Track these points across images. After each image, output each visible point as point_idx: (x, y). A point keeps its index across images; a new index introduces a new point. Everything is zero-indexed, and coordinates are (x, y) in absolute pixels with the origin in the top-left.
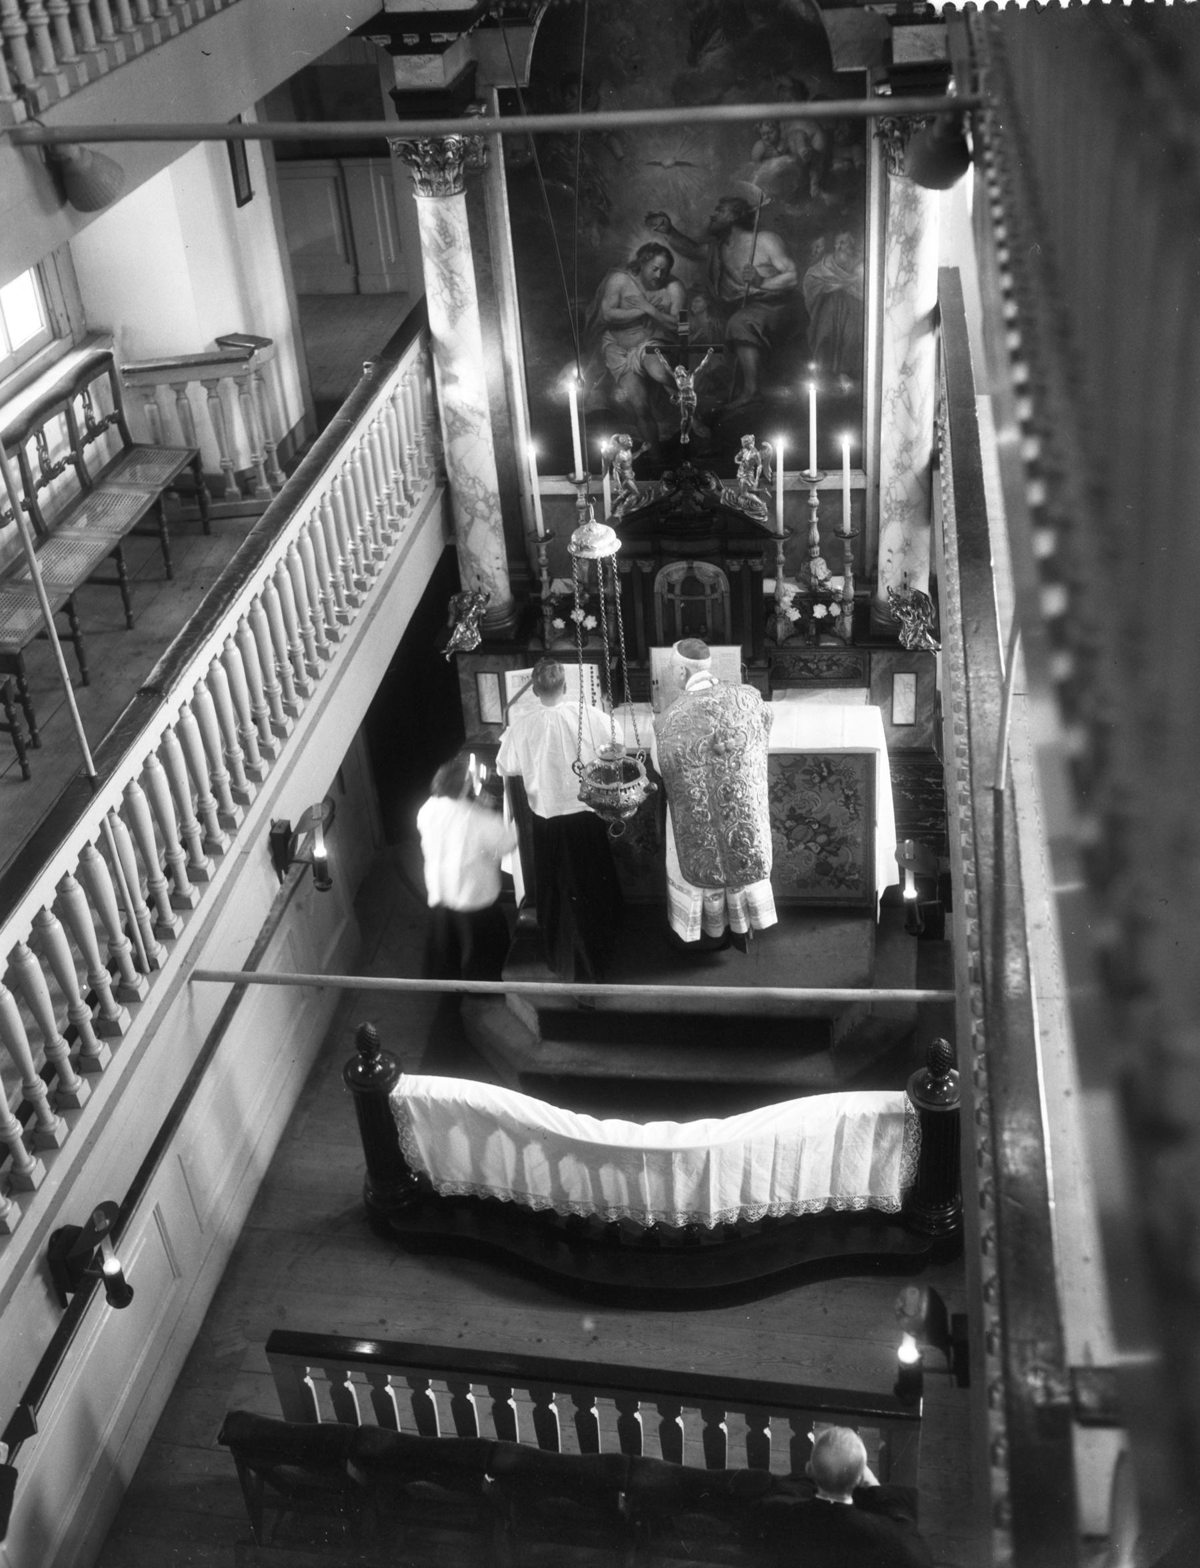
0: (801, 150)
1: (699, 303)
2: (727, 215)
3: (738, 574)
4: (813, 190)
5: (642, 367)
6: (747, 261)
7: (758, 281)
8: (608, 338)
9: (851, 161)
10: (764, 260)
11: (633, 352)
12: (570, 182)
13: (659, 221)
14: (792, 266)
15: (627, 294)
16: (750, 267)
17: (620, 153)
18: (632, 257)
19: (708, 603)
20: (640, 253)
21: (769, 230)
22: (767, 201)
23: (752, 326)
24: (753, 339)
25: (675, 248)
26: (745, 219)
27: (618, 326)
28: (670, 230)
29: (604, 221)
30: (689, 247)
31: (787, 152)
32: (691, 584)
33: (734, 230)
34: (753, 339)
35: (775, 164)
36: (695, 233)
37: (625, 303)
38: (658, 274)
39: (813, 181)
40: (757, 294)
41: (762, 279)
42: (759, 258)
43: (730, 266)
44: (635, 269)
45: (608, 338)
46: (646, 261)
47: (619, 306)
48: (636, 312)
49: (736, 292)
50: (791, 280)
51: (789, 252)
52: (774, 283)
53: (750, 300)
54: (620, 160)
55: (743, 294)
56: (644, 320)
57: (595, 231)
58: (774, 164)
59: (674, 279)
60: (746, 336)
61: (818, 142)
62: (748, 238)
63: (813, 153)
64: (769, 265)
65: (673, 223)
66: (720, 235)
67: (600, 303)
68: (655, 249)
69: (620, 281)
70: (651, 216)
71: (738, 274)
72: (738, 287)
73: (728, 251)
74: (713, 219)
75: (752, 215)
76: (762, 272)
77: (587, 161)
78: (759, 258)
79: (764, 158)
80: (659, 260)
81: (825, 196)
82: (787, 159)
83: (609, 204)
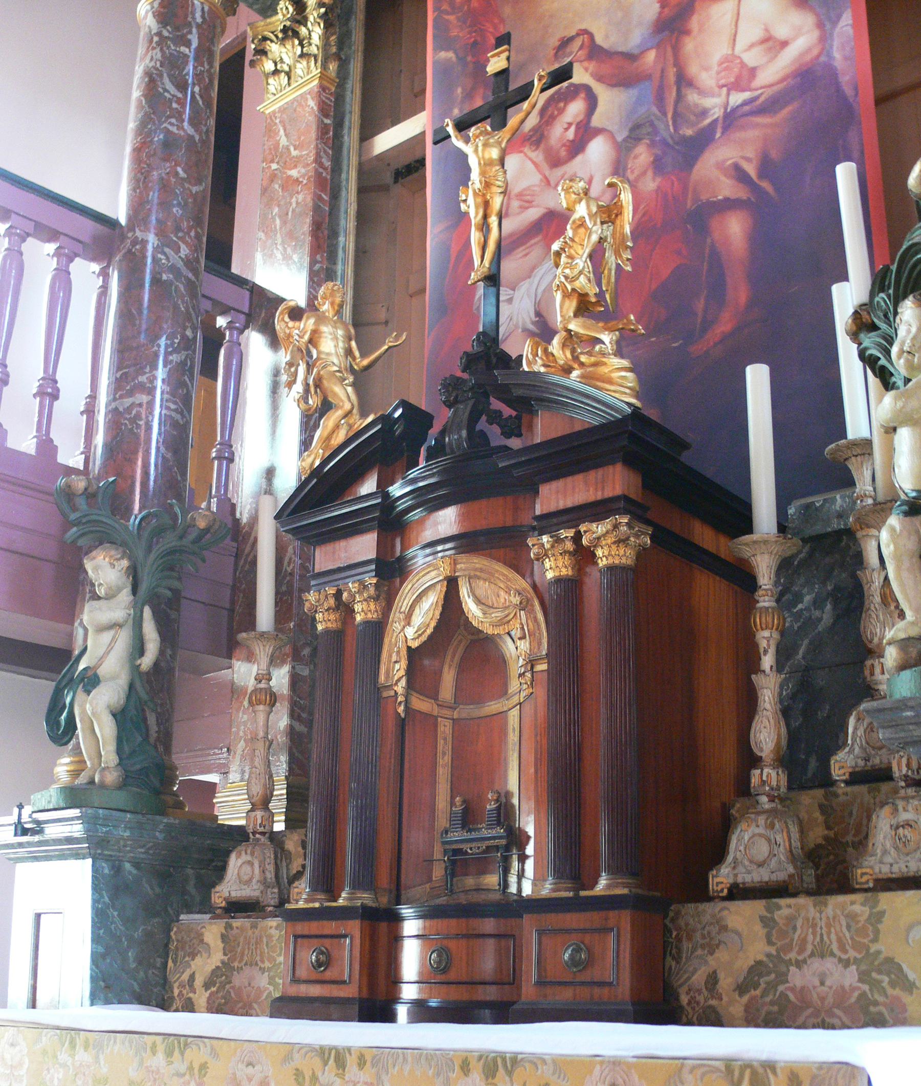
1: (642, 156)
5: (538, 314)
7: (743, 77)
10: (757, 33)
13: (578, 43)
23: (737, 167)
25: (600, 79)
30: (620, 68)
38: (571, 134)
40: (745, 103)
41: (753, 72)
43: (693, 69)
49: (704, 113)
50: (809, 50)
55: (717, 113)
59: (598, 131)
60: (727, 189)
65: (599, 40)
71: (707, 79)
72: (708, 102)
76: (751, 58)
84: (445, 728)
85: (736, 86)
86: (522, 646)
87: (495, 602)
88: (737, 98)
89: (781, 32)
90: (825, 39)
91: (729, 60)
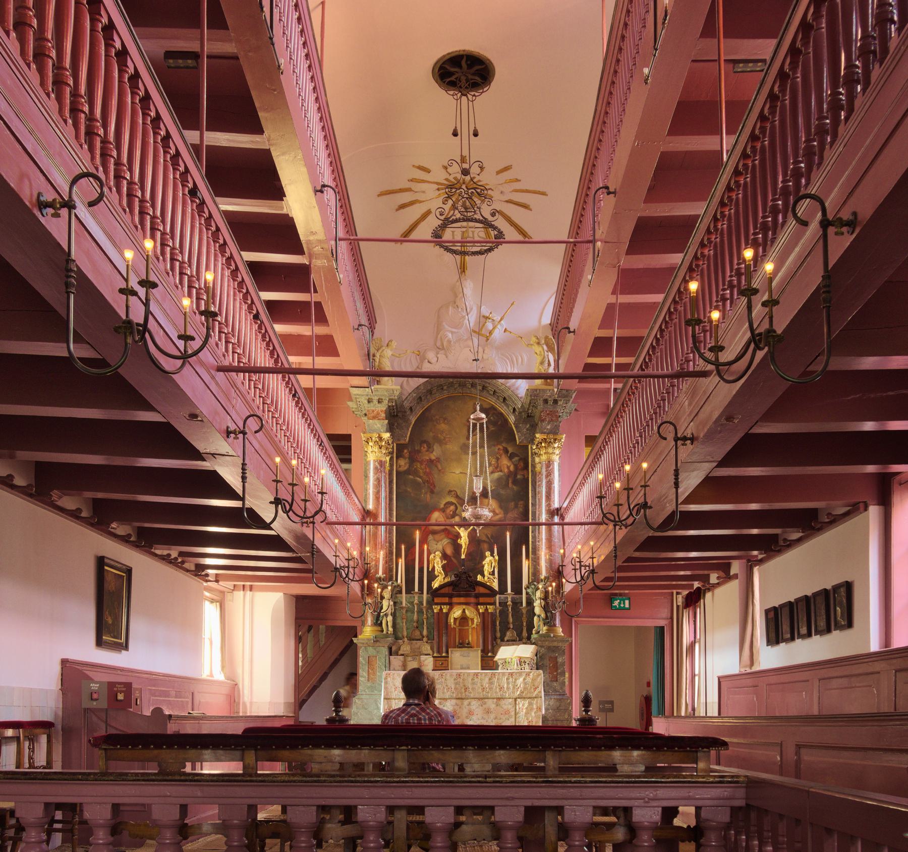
0: (506, 470)
4: (510, 485)
8: (430, 537)
12: (420, 477)
18: (442, 506)
28: (457, 497)
29: (432, 492)
32: (464, 619)
35: (496, 475)
44: (443, 510)
45: (430, 537)
51: (501, 507)
60: (484, 538)
61: (512, 468)
63: (510, 472)
68: (452, 503)
70: (450, 491)
80: (452, 508)
89: (497, 511)
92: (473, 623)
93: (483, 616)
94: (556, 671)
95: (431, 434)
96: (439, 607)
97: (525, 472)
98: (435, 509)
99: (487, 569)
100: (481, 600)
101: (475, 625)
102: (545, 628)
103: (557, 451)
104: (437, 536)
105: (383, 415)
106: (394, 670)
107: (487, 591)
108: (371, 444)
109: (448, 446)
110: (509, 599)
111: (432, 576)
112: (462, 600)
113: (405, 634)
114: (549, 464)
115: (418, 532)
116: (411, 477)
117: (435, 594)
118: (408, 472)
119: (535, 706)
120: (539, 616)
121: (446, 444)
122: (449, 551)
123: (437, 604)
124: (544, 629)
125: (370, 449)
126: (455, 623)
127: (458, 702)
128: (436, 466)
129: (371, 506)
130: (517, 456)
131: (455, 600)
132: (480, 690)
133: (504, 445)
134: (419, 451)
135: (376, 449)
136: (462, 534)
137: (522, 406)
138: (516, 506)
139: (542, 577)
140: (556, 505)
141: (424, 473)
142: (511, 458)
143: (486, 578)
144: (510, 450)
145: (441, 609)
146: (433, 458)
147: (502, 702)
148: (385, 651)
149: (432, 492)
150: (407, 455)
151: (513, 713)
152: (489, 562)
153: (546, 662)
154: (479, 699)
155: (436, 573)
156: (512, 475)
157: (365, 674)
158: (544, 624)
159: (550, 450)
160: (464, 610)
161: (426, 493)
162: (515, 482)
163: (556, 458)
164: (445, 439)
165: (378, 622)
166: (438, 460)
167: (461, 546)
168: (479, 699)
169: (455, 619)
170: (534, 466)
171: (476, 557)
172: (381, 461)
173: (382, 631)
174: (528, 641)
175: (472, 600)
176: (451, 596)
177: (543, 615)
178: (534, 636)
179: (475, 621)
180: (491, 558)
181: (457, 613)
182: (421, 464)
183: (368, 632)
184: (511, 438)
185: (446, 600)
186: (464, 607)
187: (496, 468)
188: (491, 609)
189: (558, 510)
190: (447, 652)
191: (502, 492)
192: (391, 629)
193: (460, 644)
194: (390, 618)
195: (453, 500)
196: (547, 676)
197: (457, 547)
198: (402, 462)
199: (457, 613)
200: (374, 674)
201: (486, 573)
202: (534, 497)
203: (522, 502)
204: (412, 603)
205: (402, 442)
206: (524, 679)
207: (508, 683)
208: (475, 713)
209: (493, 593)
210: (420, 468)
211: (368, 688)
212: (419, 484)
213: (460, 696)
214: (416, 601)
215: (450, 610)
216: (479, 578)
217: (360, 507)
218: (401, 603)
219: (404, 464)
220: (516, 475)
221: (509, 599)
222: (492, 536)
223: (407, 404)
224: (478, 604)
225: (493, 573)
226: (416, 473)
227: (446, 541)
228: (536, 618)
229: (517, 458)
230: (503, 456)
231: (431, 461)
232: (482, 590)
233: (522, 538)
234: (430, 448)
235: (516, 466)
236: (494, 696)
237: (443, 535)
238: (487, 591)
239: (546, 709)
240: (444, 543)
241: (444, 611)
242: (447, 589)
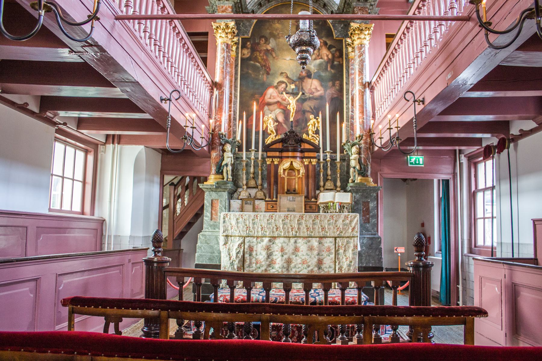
0: (326, 58)
2: (304, 73)
3: (308, 165)
4: (329, 69)
6: (309, 87)
8: (266, 108)
9: (339, 62)
10: (315, 87)
11: (273, 112)
12: (259, 62)
14: (323, 89)
15: (273, 95)
16: (310, 89)
17: (274, 55)
18: (275, 84)
19: (297, 179)
20: (278, 83)
21: (316, 79)
22: (316, 71)
24: (311, 110)
26: (309, 76)
27: (269, 104)
28: (287, 77)
29: (268, 74)
31: (322, 58)
33: (306, 78)
34: (311, 110)
35: (318, 61)
36: (295, 79)
37: (272, 97)
38: (283, 89)
39: (329, 67)
41: (314, 93)
42: (313, 87)
44: (276, 87)
45: (266, 108)
46: (279, 85)
47: (270, 98)
48: (275, 100)
51: (322, 85)
52: (317, 94)
53: (310, 98)
54: (274, 58)
56: (278, 102)
57: (265, 76)
58: (318, 61)
60: (308, 109)
61: (330, 56)
62: (309, 81)
63: (329, 59)
64: (316, 89)
66: (301, 79)
67: (264, 97)
68: (283, 82)
69: (271, 91)
70: (282, 73)
73: (304, 84)
74: (300, 75)
75: (311, 75)
76: (314, 90)
77: (265, 57)
78: (313, 87)
79: (315, 59)
80: (284, 85)
81: (333, 71)
82: (321, 60)
83: (270, 69)
84: (286, 179)
85: (311, 94)
86: (302, 171)
87: (297, 164)
88: (311, 96)
89: (319, 88)
90: (325, 93)
91: (310, 89)
92: (299, 174)
93: (307, 167)
94: (368, 214)
95: (268, 31)
96: (271, 160)
97: (341, 59)
98: (270, 86)
99: (311, 129)
100: (306, 154)
101: (300, 176)
102: (359, 178)
103: (368, 37)
104: (271, 107)
105: (230, 10)
106: (233, 211)
107: (311, 147)
108: (220, 31)
109: (281, 40)
110: (328, 156)
111: (265, 134)
112: (290, 154)
113: (245, 182)
114: (361, 46)
115: (255, 103)
116: (252, 62)
117: (267, 148)
118: (249, 59)
119: (352, 245)
120: (354, 168)
121: (279, 38)
122: (281, 119)
123: (268, 157)
124: (358, 179)
125: (218, 36)
126: (284, 174)
127: (286, 240)
128: (272, 55)
129: (217, 79)
130: (334, 47)
131: (285, 154)
132: (305, 230)
133: (324, 39)
134: (259, 44)
135: (223, 35)
136: (291, 102)
137: (338, 9)
138: (334, 85)
139: (357, 136)
140: (367, 79)
141: (262, 59)
142: (329, 48)
143: (310, 136)
144: (329, 43)
145: (273, 162)
146: (269, 48)
147: (324, 240)
148: (225, 195)
149: (268, 74)
150: (249, 46)
151: (333, 251)
152: (313, 124)
153: (361, 207)
154: (304, 237)
155: (269, 131)
156: (331, 61)
157: (209, 214)
158: (359, 174)
159: (362, 36)
160: (292, 162)
161: (263, 74)
162: (333, 67)
163: (366, 42)
164: (278, 34)
165: (219, 172)
166: (273, 50)
167: (289, 111)
168: (304, 237)
169: (284, 170)
170: (347, 55)
171: (302, 120)
172: (227, 44)
173: (223, 179)
174: (344, 189)
175: (298, 154)
176: (281, 151)
177: (358, 167)
178: (350, 184)
179: (301, 172)
180: (315, 120)
181: (286, 164)
182: (260, 53)
183: (212, 180)
184: (329, 34)
185: (277, 154)
186: (292, 160)
187: (318, 56)
188: (314, 161)
189: (369, 83)
190: (277, 198)
191: (323, 74)
192: (230, 177)
193: (288, 190)
194: (230, 168)
195: (285, 80)
196: (362, 217)
197: (286, 112)
198: (246, 51)
199: (286, 164)
200: (216, 214)
201: (310, 133)
202: (348, 78)
203: (338, 82)
204: (250, 158)
205: (246, 36)
206: (343, 221)
207: (329, 224)
208: (301, 250)
209: (316, 149)
210: (260, 56)
211: (211, 226)
212: (258, 68)
213: (287, 235)
214: (253, 157)
215: (280, 163)
216: (305, 136)
217: (209, 80)
218: (242, 158)
219: (247, 53)
220: (333, 62)
221: (328, 156)
222: (314, 107)
223: (250, 7)
224: (302, 158)
225: (317, 132)
226: (256, 60)
227: (278, 111)
228: (352, 170)
229: (334, 49)
230: (324, 47)
231: (267, 50)
232: (307, 146)
233: (338, 105)
234: (267, 41)
235: (333, 55)
236: (317, 235)
237: (276, 106)
238: (311, 147)
239: (361, 247)
240: (277, 112)
241: (276, 163)
242: (278, 144)
